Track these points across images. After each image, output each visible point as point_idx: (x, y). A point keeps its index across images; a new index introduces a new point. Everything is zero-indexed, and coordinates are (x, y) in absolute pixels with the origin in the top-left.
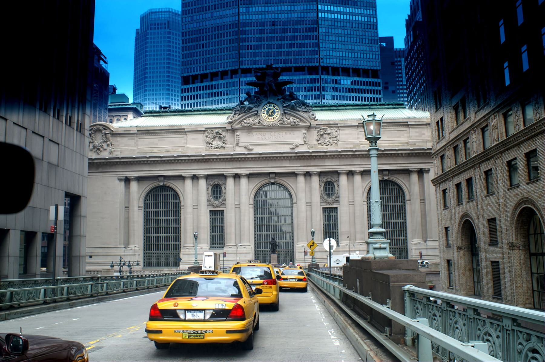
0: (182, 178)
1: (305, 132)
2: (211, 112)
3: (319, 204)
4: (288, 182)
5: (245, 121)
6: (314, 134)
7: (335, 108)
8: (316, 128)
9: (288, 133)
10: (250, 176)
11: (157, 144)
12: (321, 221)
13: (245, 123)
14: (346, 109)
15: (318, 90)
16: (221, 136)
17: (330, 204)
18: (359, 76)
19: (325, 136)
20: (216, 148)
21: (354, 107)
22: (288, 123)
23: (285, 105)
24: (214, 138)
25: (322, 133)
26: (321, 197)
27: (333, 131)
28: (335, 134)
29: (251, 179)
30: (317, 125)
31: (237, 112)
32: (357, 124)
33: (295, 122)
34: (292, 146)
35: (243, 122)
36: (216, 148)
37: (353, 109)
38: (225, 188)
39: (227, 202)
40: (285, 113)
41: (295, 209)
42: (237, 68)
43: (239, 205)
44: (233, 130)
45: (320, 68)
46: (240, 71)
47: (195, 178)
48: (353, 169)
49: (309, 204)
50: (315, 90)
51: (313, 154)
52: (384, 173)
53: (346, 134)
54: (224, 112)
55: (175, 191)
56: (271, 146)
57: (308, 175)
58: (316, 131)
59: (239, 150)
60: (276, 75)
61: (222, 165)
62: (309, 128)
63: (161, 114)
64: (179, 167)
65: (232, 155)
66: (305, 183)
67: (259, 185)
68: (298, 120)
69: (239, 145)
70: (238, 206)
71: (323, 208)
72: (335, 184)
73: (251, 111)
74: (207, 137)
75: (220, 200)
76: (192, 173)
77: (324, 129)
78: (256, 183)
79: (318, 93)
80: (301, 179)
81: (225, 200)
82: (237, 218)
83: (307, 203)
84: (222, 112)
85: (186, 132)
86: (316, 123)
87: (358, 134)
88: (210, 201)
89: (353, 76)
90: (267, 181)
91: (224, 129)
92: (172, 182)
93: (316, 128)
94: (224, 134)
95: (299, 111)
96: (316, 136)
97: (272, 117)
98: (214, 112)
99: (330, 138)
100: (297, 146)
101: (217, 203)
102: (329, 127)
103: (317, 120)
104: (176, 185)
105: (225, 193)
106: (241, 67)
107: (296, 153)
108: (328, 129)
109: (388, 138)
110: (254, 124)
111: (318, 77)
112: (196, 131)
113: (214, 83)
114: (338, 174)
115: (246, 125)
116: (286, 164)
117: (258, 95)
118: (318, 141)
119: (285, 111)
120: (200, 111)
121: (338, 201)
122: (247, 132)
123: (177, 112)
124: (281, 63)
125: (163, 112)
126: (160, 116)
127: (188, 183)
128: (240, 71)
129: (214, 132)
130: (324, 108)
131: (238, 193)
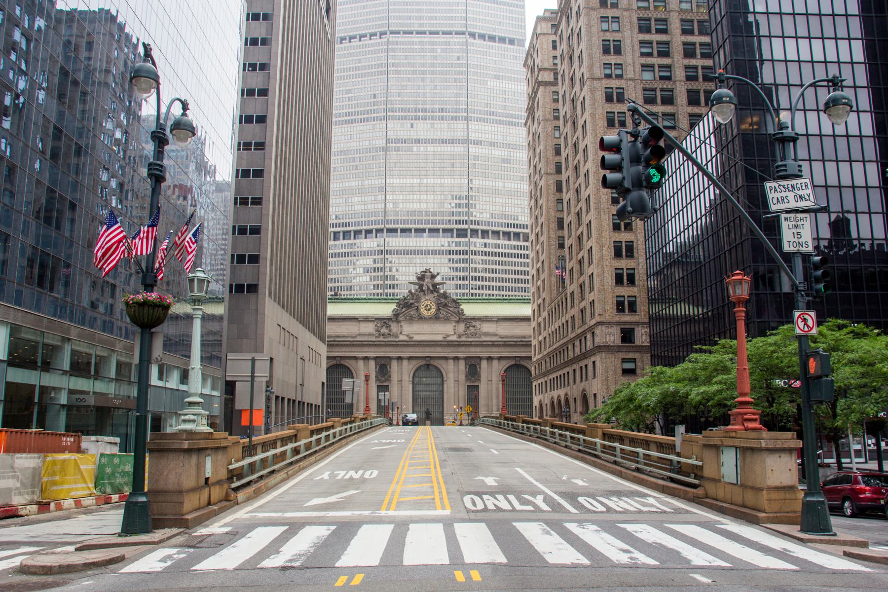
0: (356, 358)
9: (441, 325)
15: (467, 254)
17: (473, 382)
18: (509, 239)
19: (471, 328)
20: (383, 335)
24: (382, 327)
26: (466, 377)
27: (477, 324)
28: (479, 327)
34: (444, 336)
38: (390, 368)
39: (392, 379)
41: (445, 386)
42: (382, 226)
44: (398, 322)
45: (469, 231)
46: (385, 231)
47: (366, 359)
49: (457, 381)
50: (463, 254)
55: (348, 368)
57: (456, 359)
60: (433, 277)
61: (388, 349)
62: (458, 322)
64: (354, 349)
66: (454, 365)
67: (417, 366)
70: (400, 381)
76: (364, 355)
79: (467, 257)
80: (451, 362)
81: (390, 377)
82: (400, 391)
86: (464, 317)
89: (503, 240)
90: (424, 362)
91: (390, 319)
100: (448, 336)
101: (383, 379)
104: (350, 364)
106: (387, 226)
107: (448, 342)
111: (467, 240)
112: (366, 319)
113: (357, 241)
114: (480, 358)
116: (439, 349)
121: (480, 380)
124: (429, 224)
127: (361, 363)
128: (385, 231)
131: (401, 372)
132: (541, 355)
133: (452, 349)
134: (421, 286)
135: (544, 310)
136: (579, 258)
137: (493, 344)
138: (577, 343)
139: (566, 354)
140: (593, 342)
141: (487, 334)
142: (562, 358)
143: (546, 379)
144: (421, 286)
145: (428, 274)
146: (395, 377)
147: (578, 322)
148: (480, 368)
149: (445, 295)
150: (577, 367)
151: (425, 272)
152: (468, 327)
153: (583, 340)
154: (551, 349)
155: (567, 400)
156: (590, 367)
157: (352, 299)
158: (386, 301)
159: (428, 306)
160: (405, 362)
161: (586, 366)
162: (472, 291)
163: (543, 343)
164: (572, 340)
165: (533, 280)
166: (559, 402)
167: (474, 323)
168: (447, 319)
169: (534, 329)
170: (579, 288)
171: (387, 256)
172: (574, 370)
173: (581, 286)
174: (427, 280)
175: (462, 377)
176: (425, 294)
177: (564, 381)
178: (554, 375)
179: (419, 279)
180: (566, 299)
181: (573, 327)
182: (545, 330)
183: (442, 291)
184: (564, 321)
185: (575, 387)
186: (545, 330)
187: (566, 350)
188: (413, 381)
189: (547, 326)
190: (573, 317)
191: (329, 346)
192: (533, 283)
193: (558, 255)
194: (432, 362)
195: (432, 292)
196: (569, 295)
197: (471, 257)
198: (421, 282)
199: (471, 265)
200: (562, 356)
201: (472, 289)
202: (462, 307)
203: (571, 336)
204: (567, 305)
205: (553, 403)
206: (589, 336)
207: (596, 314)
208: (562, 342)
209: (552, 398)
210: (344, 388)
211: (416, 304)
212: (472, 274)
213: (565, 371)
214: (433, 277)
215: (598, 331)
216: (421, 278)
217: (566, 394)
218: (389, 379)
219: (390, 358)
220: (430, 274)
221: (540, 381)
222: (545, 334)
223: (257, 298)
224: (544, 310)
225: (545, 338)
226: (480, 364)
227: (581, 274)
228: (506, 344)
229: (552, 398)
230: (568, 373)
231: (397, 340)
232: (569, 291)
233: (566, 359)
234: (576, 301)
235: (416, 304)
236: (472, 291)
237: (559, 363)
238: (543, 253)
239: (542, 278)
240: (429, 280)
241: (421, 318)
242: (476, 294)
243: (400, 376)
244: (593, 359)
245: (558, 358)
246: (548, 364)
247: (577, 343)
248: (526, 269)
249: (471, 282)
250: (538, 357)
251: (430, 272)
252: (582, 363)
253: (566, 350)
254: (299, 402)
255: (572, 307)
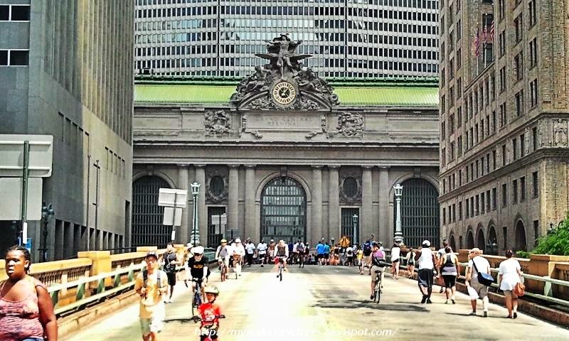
1: (324, 118)
2: (206, 82)
3: (338, 203)
4: (302, 177)
5: (253, 102)
6: (335, 119)
7: (362, 84)
8: (337, 113)
10: (257, 168)
11: (145, 125)
12: (338, 224)
13: (254, 105)
14: (375, 86)
15: (342, 14)
16: (224, 118)
20: (217, 133)
21: (385, 84)
22: (305, 108)
23: (301, 84)
24: (215, 121)
25: (344, 120)
28: (360, 122)
29: (258, 172)
30: (338, 110)
31: (243, 90)
32: (387, 111)
33: (313, 107)
34: (308, 135)
35: (250, 104)
36: (217, 133)
37: (385, 86)
38: (228, 182)
40: (302, 95)
41: (309, 209)
43: (244, 201)
44: (239, 113)
48: (379, 165)
49: (326, 202)
51: (333, 146)
52: (415, 169)
53: (372, 122)
54: (224, 82)
56: (283, 134)
57: (325, 169)
58: (338, 117)
59: (246, 137)
62: (328, 114)
63: (142, 81)
65: (238, 143)
68: (316, 104)
69: (246, 131)
71: (342, 209)
72: (357, 181)
73: (261, 90)
74: (206, 119)
75: (221, 195)
77: (346, 115)
78: (266, 176)
80: (318, 173)
83: (323, 202)
84: (220, 82)
85: (181, 112)
86: (338, 107)
87: (387, 123)
88: (209, 196)
90: (278, 174)
91: (227, 110)
92: (164, 171)
93: (337, 113)
94: (227, 116)
95: (318, 92)
96: (337, 124)
97: (286, 99)
98: (210, 82)
99: (354, 127)
100: (314, 135)
102: (352, 114)
103: (338, 104)
105: (227, 187)
108: (352, 115)
109: (422, 128)
110: (264, 107)
112: (193, 110)
114: (362, 169)
115: (254, 107)
116: (301, 155)
117: (269, 70)
118: (339, 129)
119: (302, 93)
120: (192, 80)
121: (360, 202)
122: (256, 115)
123: (162, 80)
125: (145, 79)
126: (141, 83)
129: (216, 113)
130: (348, 83)
132: (454, 164)
133: (319, 154)
134: (274, 60)
135: (459, 96)
136: (515, 17)
137: (380, 148)
138: (509, 145)
139: (492, 161)
140: (535, 143)
141: (372, 133)
142: (486, 168)
143: (460, 199)
144: (274, 60)
145: (285, 42)
146: (234, 194)
147: (511, 113)
148: (361, 182)
149: (309, 75)
150: (508, 180)
151: (281, 39)
152: (344, 123)
153: (519, 141)
154: (469, 154)
155: (492, 231)
156: (529, 183)
157: (170, 79)
158: (220, 81)
159: (283, 89)
160: (250, 173)
161: (523, 179)
162: (349, 70)
163: (456, 145)
164: (501, 143)
165: (443, 51)
166: (481, 233)
167: (352, 117)
168: (312, 112)
169: (443, 124)
170: (514, 62)
171: (222, 16)
172: (504, 186)
173: (517, 59)
174: (284, 52)
175: (335, 197)
176: (279, 72)
177: (489, 202)
178: (473, 194)
179: (271, 49)
180: (493, 79)
181: (504, 121)
182: (460, 126)
183: (305, 69)
184: (489, 112)
185: (504, 210)
186: (460, 126)
187: (491, 156)
188: (261, 201)
189: (463, 120)
190: (503, 107)
191: (137, 148)
192: (443, 55)
193: (482, 12)
194: (289, 174)
195: (290, 70)
196: (498, 72)
197: (349, 18)
198: (275, 55)
199: (349, 31)
200: (486, 165)
201: (350, 66)
202: (334, 92)
203: (500, 135)
204: (494, 88)
205: (471, 234)
206: (528, 134)
207: (540, 102)
208: (485, 144)
209: (470, 227)
210: (161, 202)
211: (267, 88)
212: (349, 44)
213: (490, 187)
214: (292, 47)
215: (542, 126)
216: (275, 48)
217: (491, 222)
218: (226, 199)
219: (227, 168)
220: (288, 43)
221: (450, 203)
222: (459, 132)
223: (27, 71)
224: (459, 96)
225: (460, 138)
226: (361, 177)
227: (518, 41)
228: (400, 149)
229: (470, 227)
230: (494, 190)
231: (238, 141)
232: (497, 68)
233: (492, 170)
234: (509, 83)
235: (267, 88)
236: (349, 70)
237: (480, 176)
238: (458, 9)
239: (456, 49)
240: (286, 51)
241: (274, 110)
242: (355, 74)
243: (242, 194)
244: (533, 169)
245: (480, 168)
246: (464, 177)
247: (509, 145)
248: (431, 36)
249: (349, 56)
250: (449, 167)
251: (288, 40)
252: (516, 176)
253: (491, 156)
254: (92, 230)
255: (502, 91)
